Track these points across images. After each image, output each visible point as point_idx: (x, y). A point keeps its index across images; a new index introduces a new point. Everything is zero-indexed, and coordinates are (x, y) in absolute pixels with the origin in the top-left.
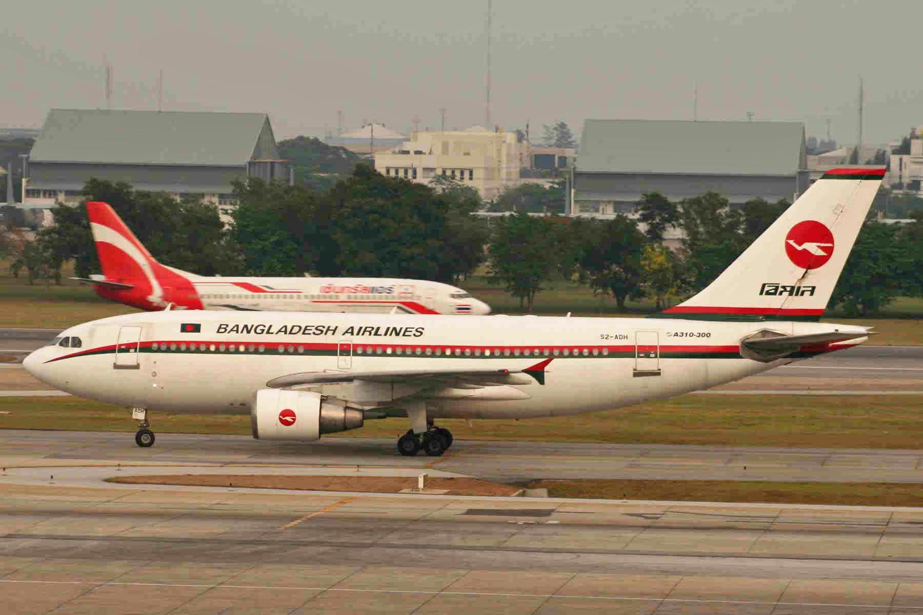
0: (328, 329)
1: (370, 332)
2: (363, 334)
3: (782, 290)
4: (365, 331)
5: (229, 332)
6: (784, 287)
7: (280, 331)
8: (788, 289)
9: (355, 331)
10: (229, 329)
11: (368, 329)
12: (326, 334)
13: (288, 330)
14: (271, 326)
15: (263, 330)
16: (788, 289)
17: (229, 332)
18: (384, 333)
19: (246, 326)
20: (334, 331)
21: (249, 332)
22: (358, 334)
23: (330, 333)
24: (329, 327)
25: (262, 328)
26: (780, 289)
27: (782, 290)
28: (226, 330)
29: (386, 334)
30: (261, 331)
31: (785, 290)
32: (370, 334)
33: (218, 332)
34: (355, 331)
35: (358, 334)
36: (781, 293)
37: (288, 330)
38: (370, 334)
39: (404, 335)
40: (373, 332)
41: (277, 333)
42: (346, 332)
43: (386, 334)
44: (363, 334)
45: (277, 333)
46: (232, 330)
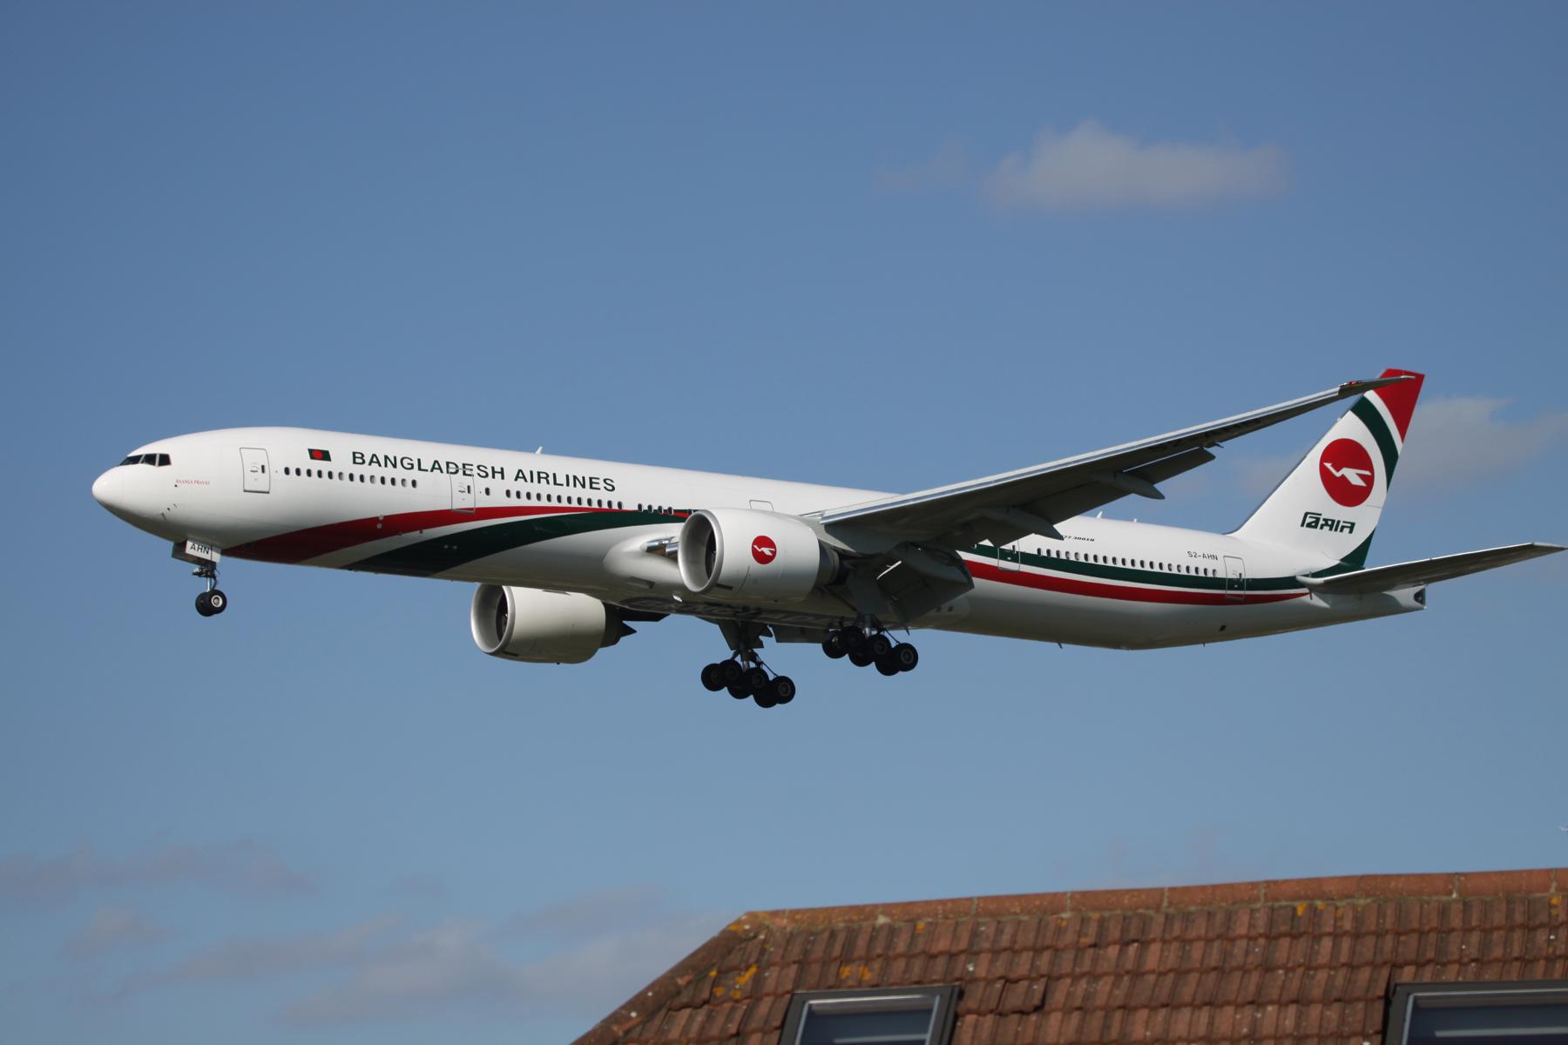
0: (494, 472)
1: (546, 478)
2: (539, 482)
3: (1324, 523)
4: (539, 478)
5: (370, 464)
6: (1324, 520)
7: (433, 468)
8: (1330, 523)
9: (528, 478)
10: (367, 459)
11: (544, 475)
12: (494, 477)
13: (444, 467)
14: (419, 460)
15: (412, 465)
16: (1330, 523)
17: (370, 464)
18: (565, 484)
19: (386, 457)
20: (502, 472)
21: (395, 466)
22: (532, 481)
23: (498, 476)
24: (493, 468)
25: (409, 461)
26: (1321, 522)
27: (1324, 523)
28: (364, 462)
29: (568, 485)
30: (410, 466)
31: (1326, 524)
32: (548, 483)
33: (355, 462)
34: (528, 477)
35: (532, 481)
36: (1322, 528)
37: (444, 467)
38: (548, 483)
39: (591, 487)
40: (551, 479)
41: (432, 471)
42: (517, 478)
43: (568, 485)
44: (539, 482)
45: (432, 471)
46: (371, 462)
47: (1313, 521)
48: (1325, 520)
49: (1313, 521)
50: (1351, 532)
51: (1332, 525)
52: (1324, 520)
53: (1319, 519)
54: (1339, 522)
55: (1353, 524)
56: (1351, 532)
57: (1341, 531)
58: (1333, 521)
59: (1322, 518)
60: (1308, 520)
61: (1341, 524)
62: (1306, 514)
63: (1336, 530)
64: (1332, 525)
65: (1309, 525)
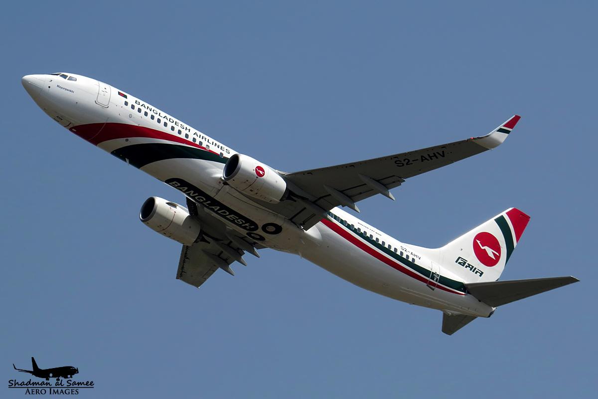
6: (468, 264)
26: (466, 264)
47: (462, 263)
48: (469, 265)
49: (462, 263)
50: (480, 276)
51: (472, 268)
52: (468, 264)
53: (465, 263)
54: (475, 268)
55: (482, 273)
56: (480, 276)
57: (476, 273)
58: (473, 267)
59: (467, 263)
60: (460, 261)
61: (476, 270)
62: (459, 258)
63: (473, 271)
64: (472, 268)
65: (460, 263)
